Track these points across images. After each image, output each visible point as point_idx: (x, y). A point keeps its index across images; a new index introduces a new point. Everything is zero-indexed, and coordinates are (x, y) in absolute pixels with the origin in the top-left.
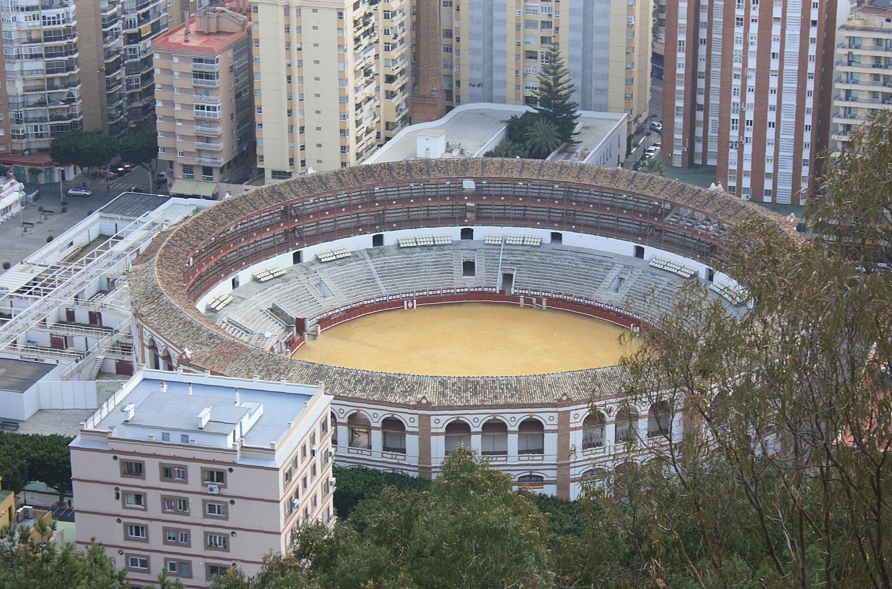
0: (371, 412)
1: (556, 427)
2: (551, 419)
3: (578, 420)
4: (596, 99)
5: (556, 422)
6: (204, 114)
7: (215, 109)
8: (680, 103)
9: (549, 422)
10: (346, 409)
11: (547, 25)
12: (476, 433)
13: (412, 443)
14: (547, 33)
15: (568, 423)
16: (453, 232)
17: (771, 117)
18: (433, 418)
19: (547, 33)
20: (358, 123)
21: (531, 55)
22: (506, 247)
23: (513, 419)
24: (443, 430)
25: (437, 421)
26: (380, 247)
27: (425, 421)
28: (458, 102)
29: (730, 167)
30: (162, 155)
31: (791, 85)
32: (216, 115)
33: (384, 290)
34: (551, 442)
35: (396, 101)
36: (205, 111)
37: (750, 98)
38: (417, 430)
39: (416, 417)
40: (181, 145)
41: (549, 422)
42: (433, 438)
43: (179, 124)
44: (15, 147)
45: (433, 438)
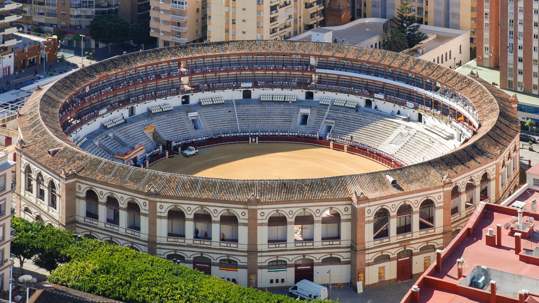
0: (119, 195)
1: (246, 222)
2: (243, 214)
3: (264, 217)
4: (452, 21)
5: (246, 217)
6: (176, 7)
7: (183, 4)
8: (486, 21)
9: (241, 217)
10: (105, 192)
12: (189, 220)
13: (144, 222)
15: (256, 219)
16: (300, 94)
18: (158, 204)
20: (273, 20)
22: (333, 107)
23: (217, 211)
24: (166, 214)
25: (161, 207)
26: (248, 99)
27: (153, 205)
28: (365, 16)
29: (509, 66)
30: (152, 34)
32: (183, 8)
33: (240, 127)
34: (243, 233)
35: (312, 10)
36: (177, 5)
38: (147, 212)
39: (147, 202)
40: (163, 28)
41: (241, 217)
42: (158, 220)
43: (162, 12)
44: (73, 23)
45: (158, 220)
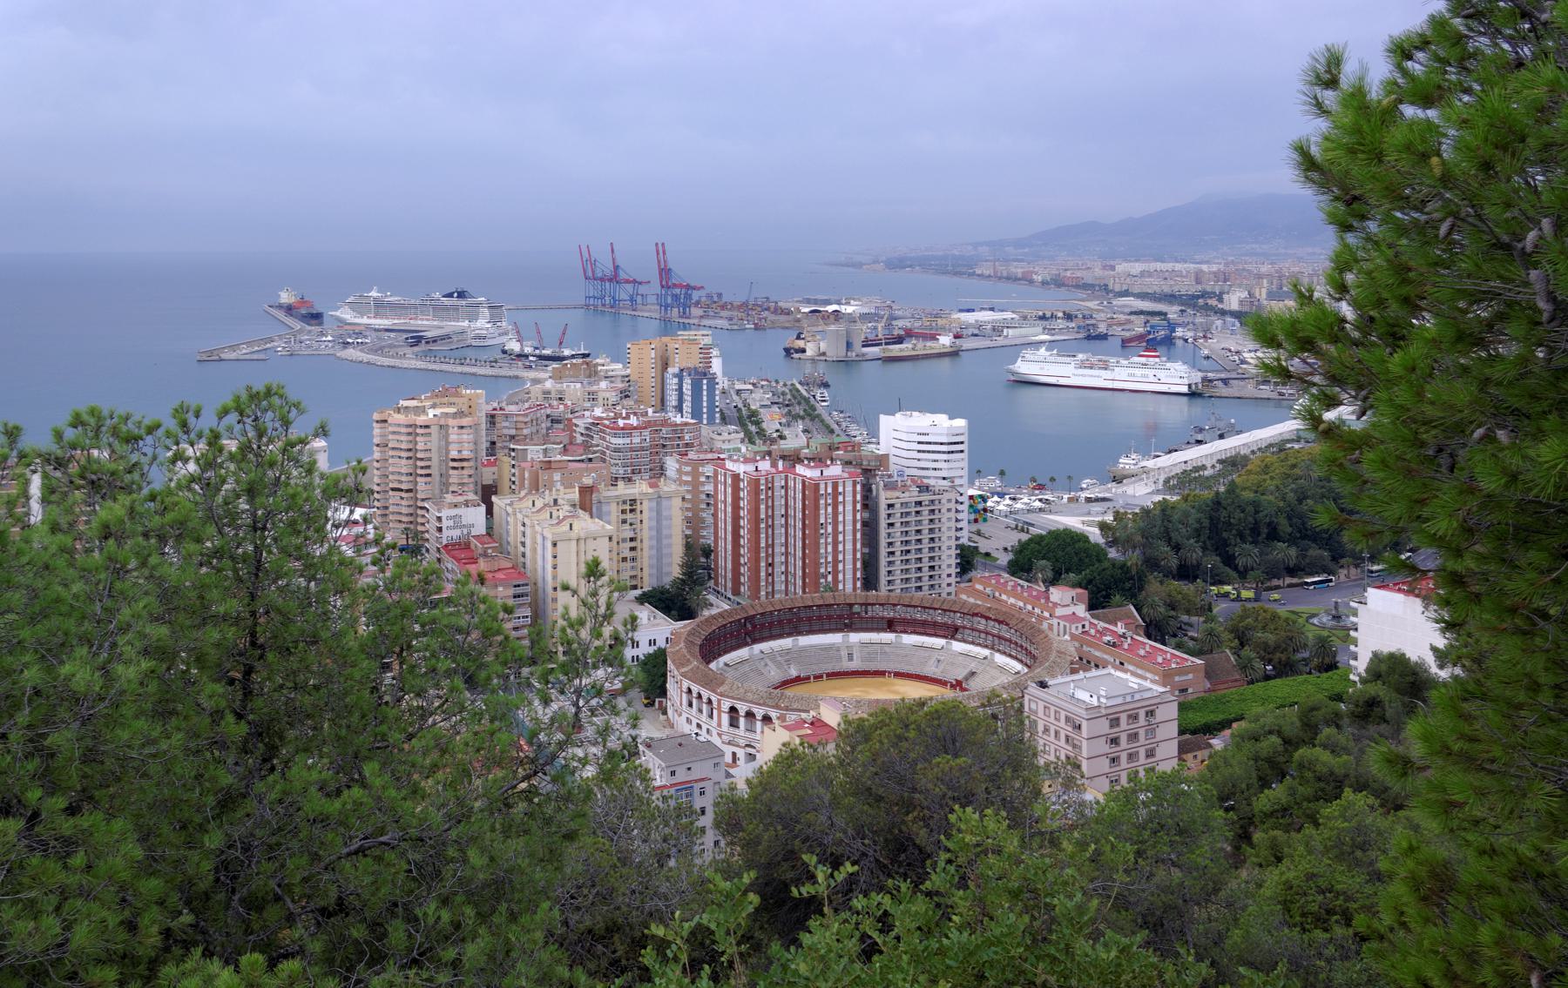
11: (632, 540)
14: (633, 544)
17: (841, 557)
19: (633, 544)
21: (624, 559)
31: (849, 537)
37: (830, 549)
